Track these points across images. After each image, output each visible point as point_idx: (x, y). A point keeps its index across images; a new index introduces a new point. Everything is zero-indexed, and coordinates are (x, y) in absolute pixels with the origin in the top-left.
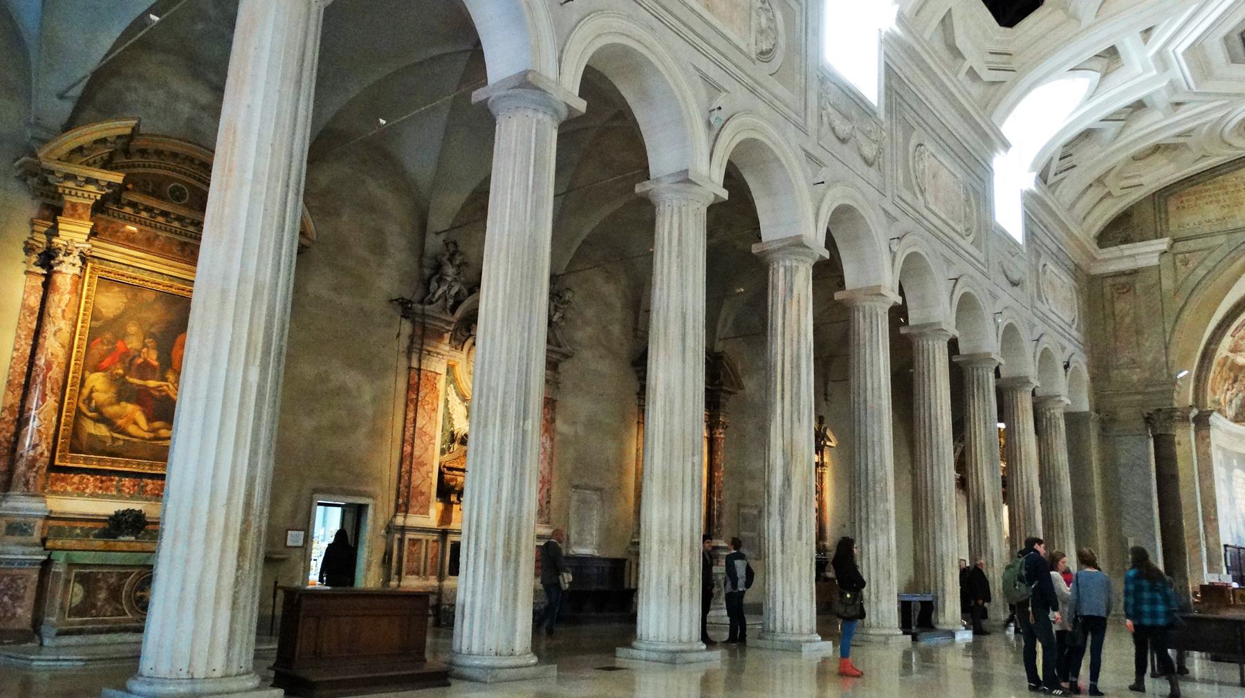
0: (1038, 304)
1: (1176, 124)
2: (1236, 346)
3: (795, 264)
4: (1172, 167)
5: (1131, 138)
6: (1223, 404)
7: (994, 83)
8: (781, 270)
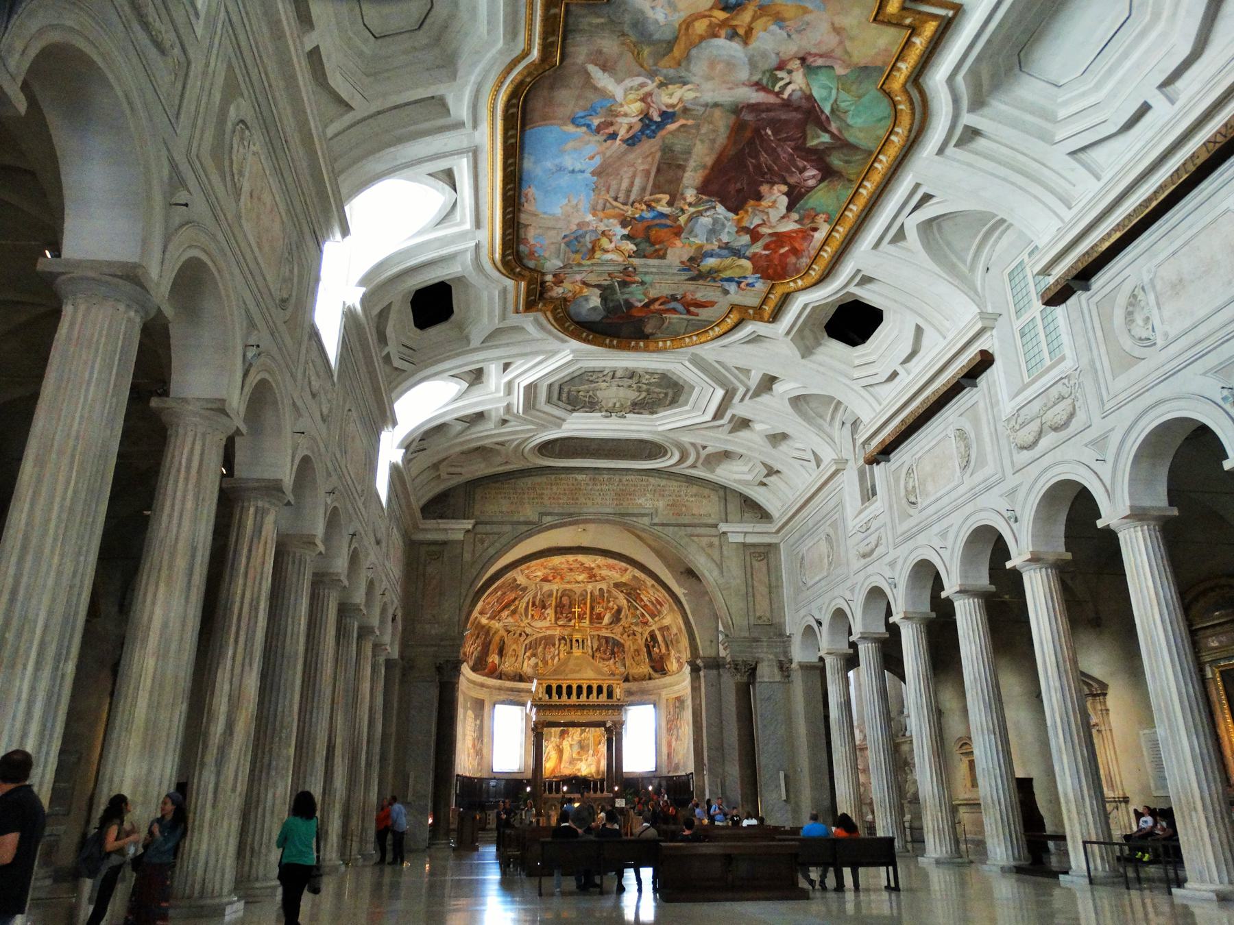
0: (386, 563)
1: (500, 435)
3: (267, 506)
4: (483, 466)
5: (468, 438)
7: (396, 369)
8: (252, 510)
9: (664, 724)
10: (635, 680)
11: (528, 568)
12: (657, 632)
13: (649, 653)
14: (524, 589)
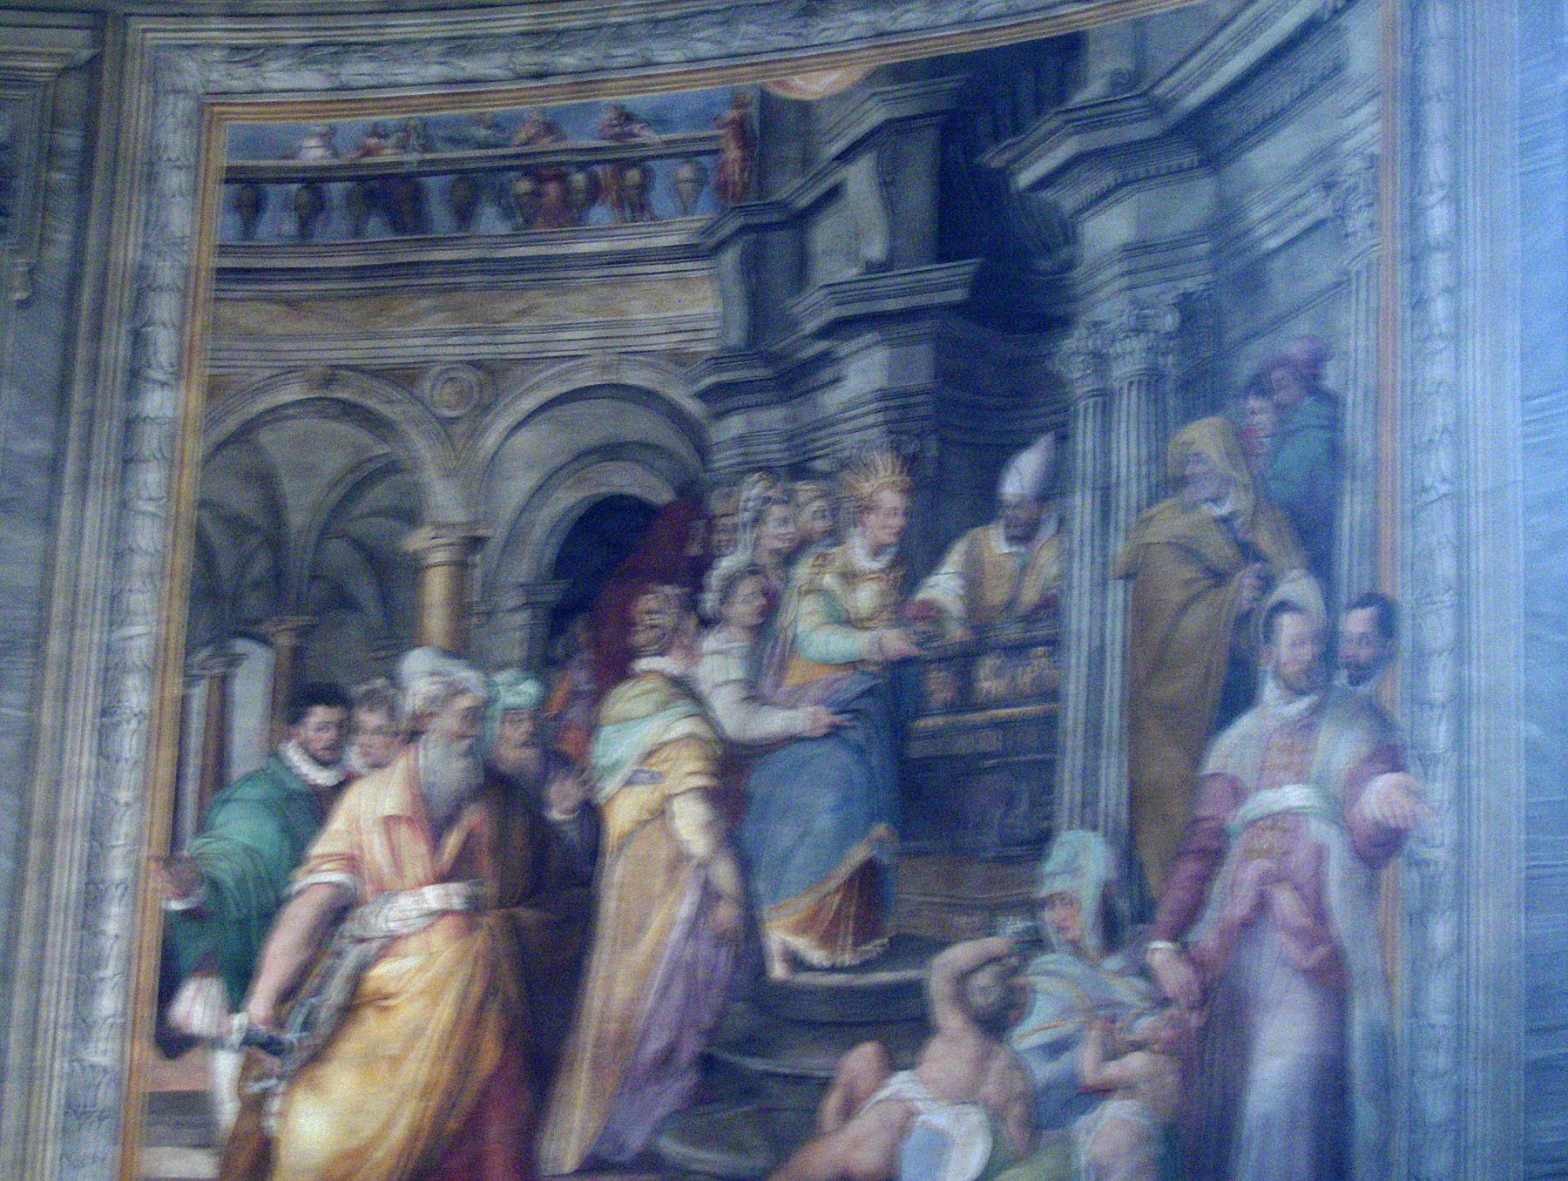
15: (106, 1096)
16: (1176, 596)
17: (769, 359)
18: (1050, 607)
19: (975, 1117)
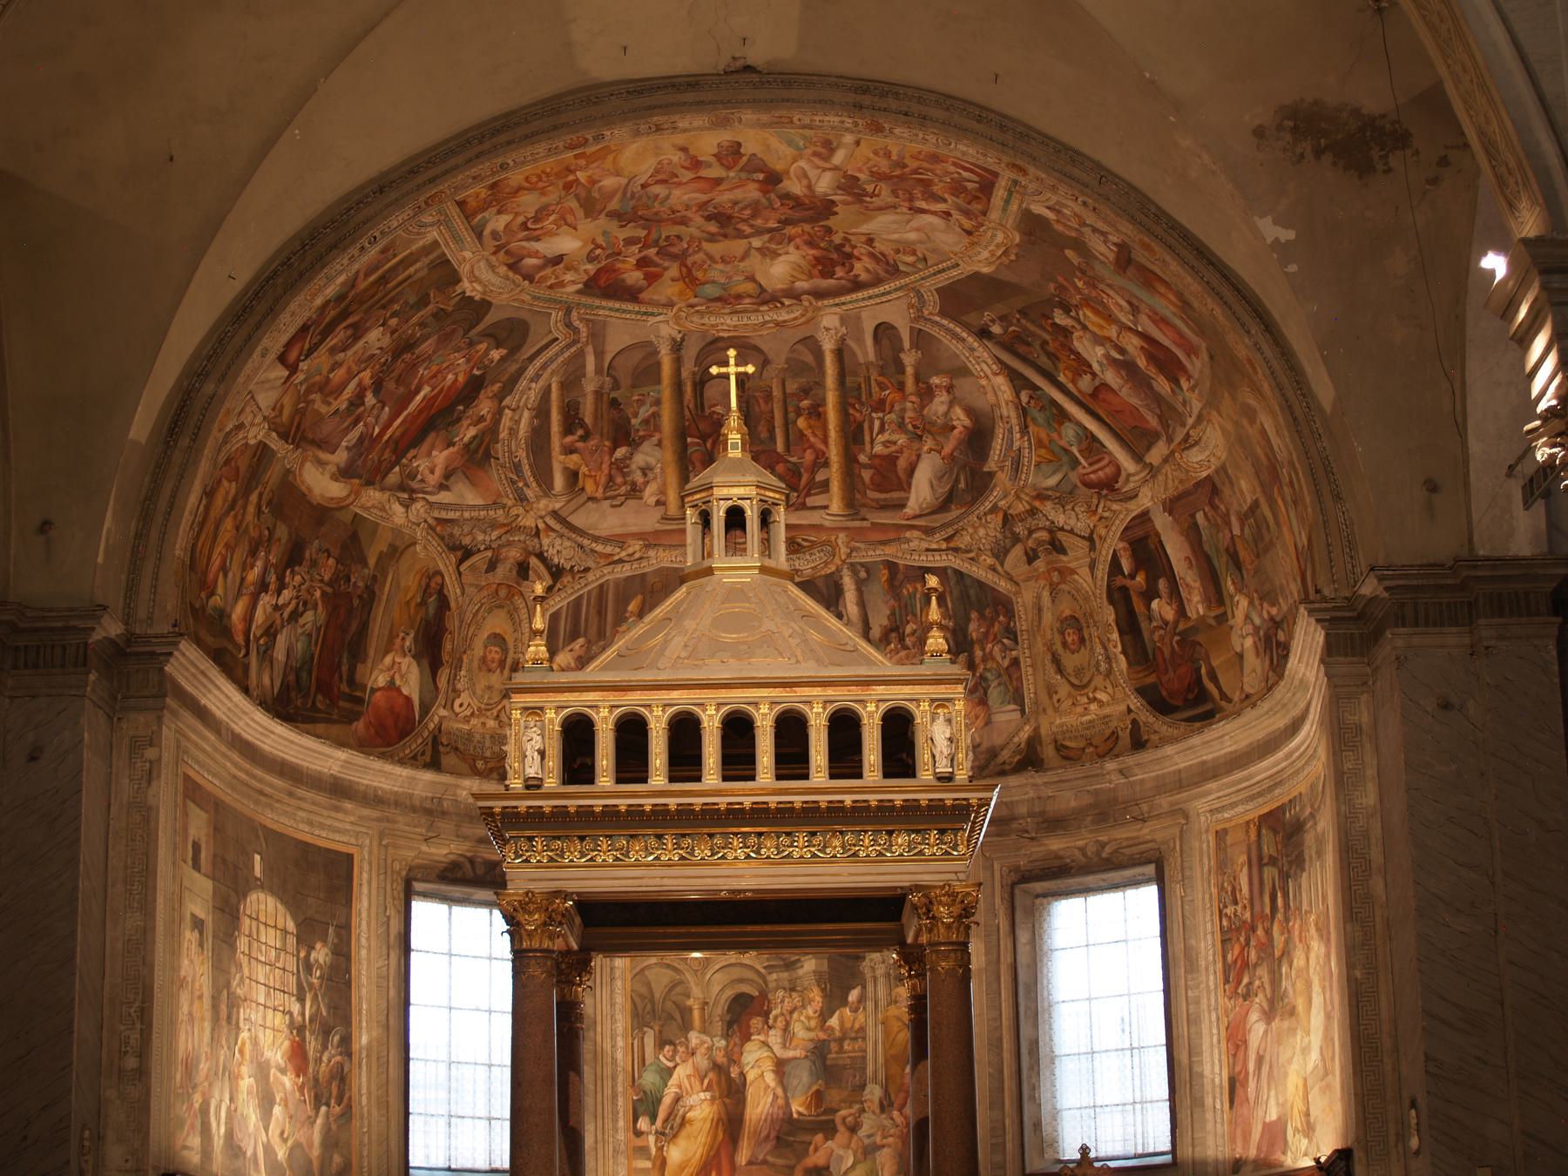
2: (299, 413)
6: (240, 639)
9: (1206, 945)
10: (1067, 755)
11: (499, 197)
12: (1162, 521)
13: (1130, 626)
14: (512, 334)
15: (623, 1147)
16: (895, 1029)
17: (784, 960)
18: (862, 1029)
19: (850, 1152)
